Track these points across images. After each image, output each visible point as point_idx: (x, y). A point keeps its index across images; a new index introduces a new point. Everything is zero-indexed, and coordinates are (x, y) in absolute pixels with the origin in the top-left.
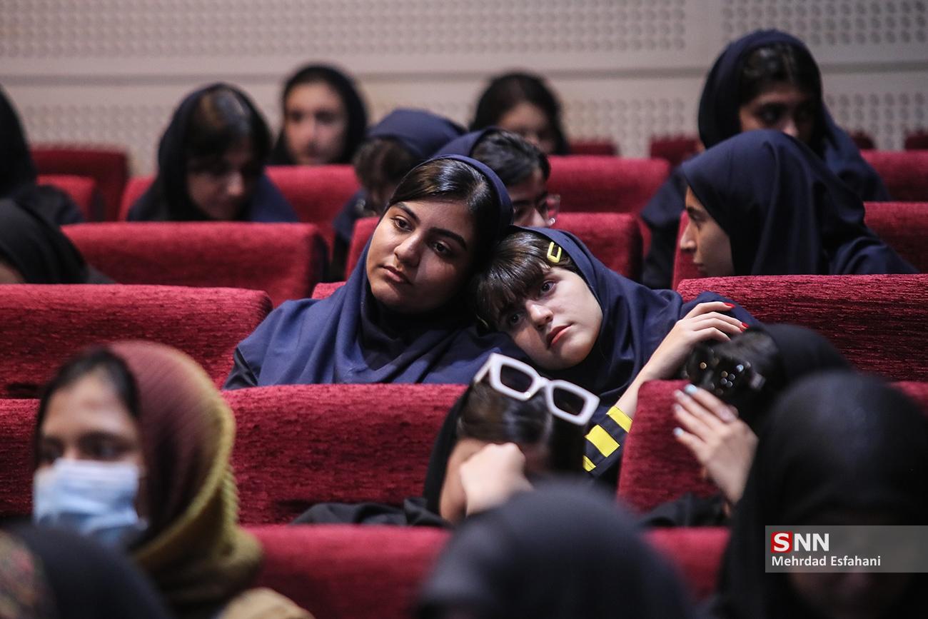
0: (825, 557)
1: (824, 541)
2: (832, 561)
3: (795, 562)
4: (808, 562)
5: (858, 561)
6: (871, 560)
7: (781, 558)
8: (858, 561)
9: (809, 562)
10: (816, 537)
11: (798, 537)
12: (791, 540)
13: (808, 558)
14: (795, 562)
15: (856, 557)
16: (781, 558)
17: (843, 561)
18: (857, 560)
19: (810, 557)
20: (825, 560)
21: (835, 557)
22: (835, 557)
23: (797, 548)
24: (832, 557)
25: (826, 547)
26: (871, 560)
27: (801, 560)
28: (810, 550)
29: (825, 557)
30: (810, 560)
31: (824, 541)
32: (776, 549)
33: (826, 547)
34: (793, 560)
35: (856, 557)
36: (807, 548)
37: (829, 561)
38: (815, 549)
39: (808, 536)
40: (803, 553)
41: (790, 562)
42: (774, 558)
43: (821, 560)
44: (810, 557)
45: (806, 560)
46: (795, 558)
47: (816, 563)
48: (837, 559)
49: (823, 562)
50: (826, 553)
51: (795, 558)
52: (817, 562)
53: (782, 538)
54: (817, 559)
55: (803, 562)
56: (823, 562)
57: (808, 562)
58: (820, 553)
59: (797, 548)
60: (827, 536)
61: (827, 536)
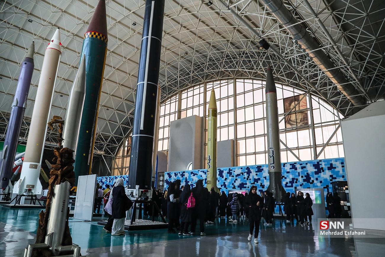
0: (342, 231)
1: (342, 224)
2: (345, 233)
3: (330, 233)
4: (335, 233)
5: (356, 233)
6: (362, 233)
7: (324, 232)
8: (356, 233)
9: (335, 233)
10: (339, 223)
11: (331, 223)
12: (328, 224)
13: (335, 232)
14: (330, 233)
15: (355, 231)
16: (324, 232)
17: (350, 233)
18: (355, 233)
19: (336, 231)
20: (342, 232)
21: (346, 231)
22: (346, 231)
23: (330, 228)
24: (345, 231)
25: (343, 227)
26: (362, 233)
27: (332, 233)
28: (336, 228)
29: (342, 231)
30: (336, 233)
31: (342, 224)
32: (322, 228)
33: (343, 227)
34: (329, 232)
35: (355, 231)
36: (335, 227)
37: (344, 233)
38: (338, 228)
39: (335, 222)
40: (333, 230)
41: (328, 233)
42: (321, 232)
43: (341, 232)
44: (336, 231)
45: (335, 232)
46: (330, 232)
47: (339, 234)
48: (347, 232)
49: (341, 233)
50: (342, 230)
51: (330, 232)
52: (339, 233)
53: (324, 223)
54: (339, 232)
55: (333, 233)
56: (341, 233)
57: (335, 233)
58: (340, 230)
59: (330, 228)
60: (343, 222)
61: (343, 222)
